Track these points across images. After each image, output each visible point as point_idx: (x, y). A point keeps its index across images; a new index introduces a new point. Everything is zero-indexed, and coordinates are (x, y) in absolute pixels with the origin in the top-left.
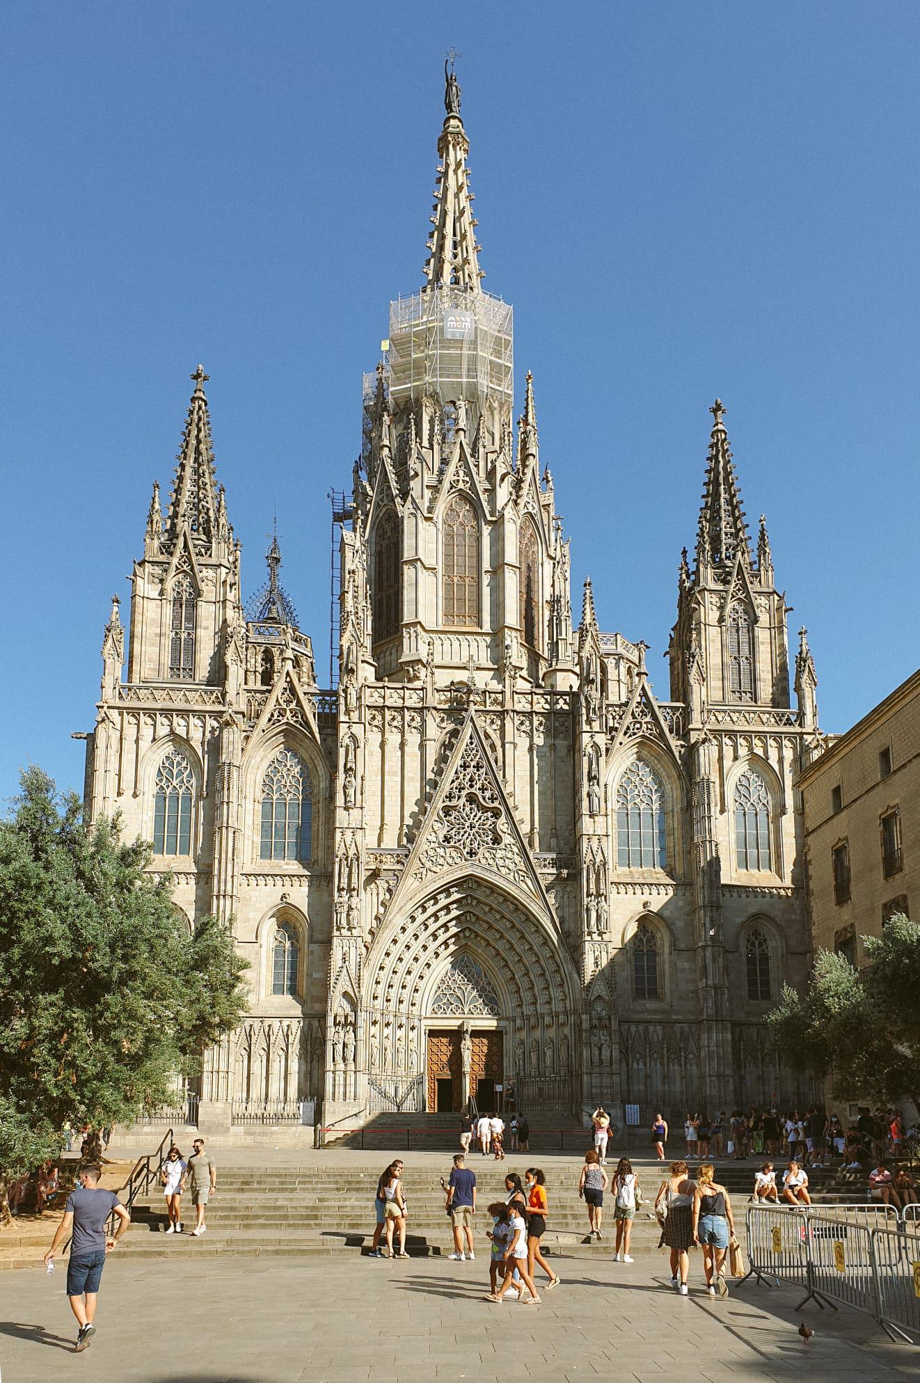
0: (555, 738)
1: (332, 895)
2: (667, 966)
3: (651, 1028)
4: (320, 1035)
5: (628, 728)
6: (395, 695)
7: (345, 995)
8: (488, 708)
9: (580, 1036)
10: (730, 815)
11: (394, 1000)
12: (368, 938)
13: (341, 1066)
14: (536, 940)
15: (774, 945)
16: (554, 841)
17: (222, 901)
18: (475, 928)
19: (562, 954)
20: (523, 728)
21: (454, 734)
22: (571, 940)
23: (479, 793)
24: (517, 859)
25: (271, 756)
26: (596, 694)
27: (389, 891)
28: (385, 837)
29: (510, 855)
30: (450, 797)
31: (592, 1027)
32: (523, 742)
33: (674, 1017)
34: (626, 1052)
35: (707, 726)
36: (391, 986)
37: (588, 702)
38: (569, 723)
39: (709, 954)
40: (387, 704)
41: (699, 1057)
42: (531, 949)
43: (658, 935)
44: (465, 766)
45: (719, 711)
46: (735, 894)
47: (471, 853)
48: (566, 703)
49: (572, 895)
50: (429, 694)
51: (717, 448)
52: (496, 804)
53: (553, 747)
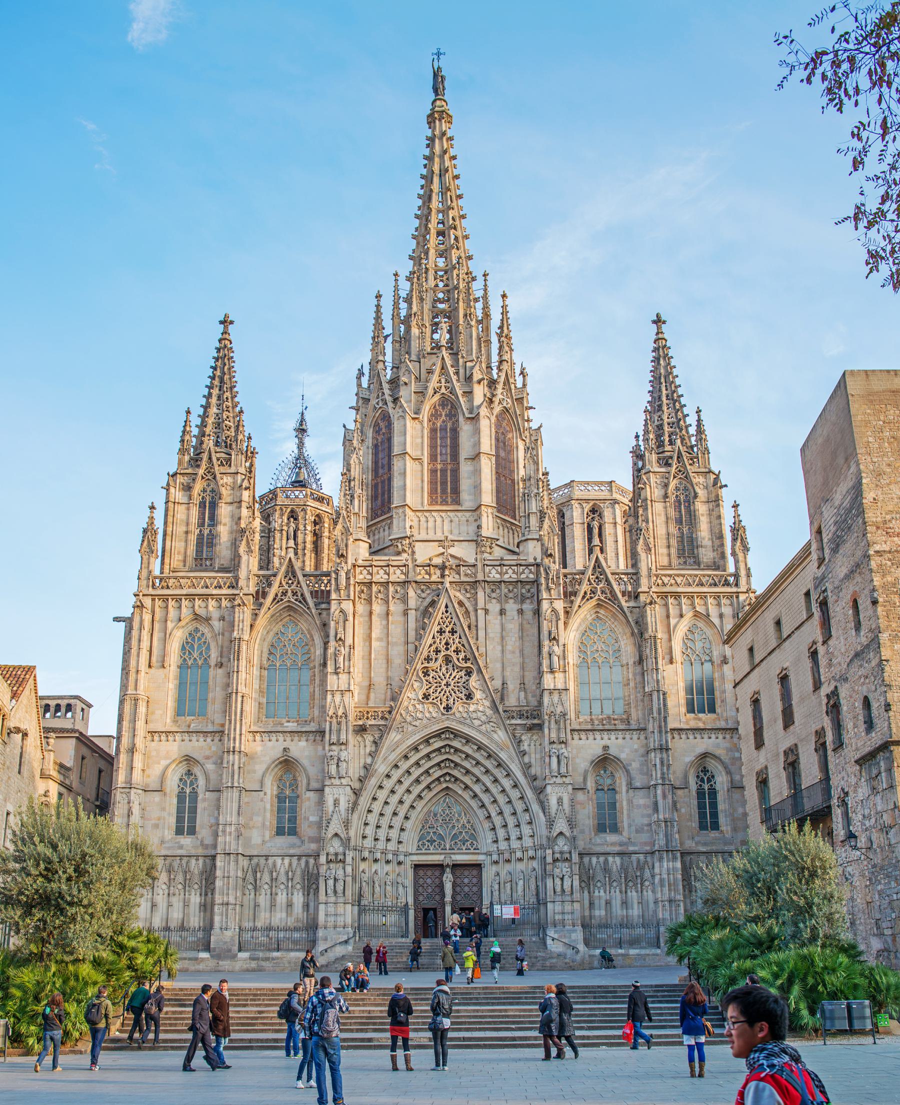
0: (522, 602)
1: (324, 749)
2: (625, 803)
3: (610, 859)
4: (315, 872)
5: (585, 593)
6: (381, 572)
7: (336, 835)
8: (464, 579)
9: (545, 869)
10: (678, 667)
11: (382, 838)
12: (357, 785)
13: (332, 899)
14: (507, 783)
15: (721, 781)
16: (522, 694)
17: (231, 756)
18: (455, 773)
19: (530, 794)
20: (494, 595)
21: (433, 603)
22: (538, 783)
23: (454, 655)
24: (489, 712)
25: (275, 630)
26: (555, 567)
27: (375, 742)
28: (372, 695)
29: (481, 709)
30: (428, 659)
31: (555, 860)
32: (494, 607)
33: (631, 848)
34: (587, 880)
35: (654, 589)
36: (378, 827)
37: (547, 574)
38: (534, 590)
39: (659, 792)
40: (374, 580)
41: (653, 884)
42: (503, 791)
43: (617, 775)
44: (441, 632)
45: (665, 575)
46: (684, 736)
47: (448, 708)
48: (531, 572)
49: (538, 744)
50: (411, 570)
53: (521, 612)
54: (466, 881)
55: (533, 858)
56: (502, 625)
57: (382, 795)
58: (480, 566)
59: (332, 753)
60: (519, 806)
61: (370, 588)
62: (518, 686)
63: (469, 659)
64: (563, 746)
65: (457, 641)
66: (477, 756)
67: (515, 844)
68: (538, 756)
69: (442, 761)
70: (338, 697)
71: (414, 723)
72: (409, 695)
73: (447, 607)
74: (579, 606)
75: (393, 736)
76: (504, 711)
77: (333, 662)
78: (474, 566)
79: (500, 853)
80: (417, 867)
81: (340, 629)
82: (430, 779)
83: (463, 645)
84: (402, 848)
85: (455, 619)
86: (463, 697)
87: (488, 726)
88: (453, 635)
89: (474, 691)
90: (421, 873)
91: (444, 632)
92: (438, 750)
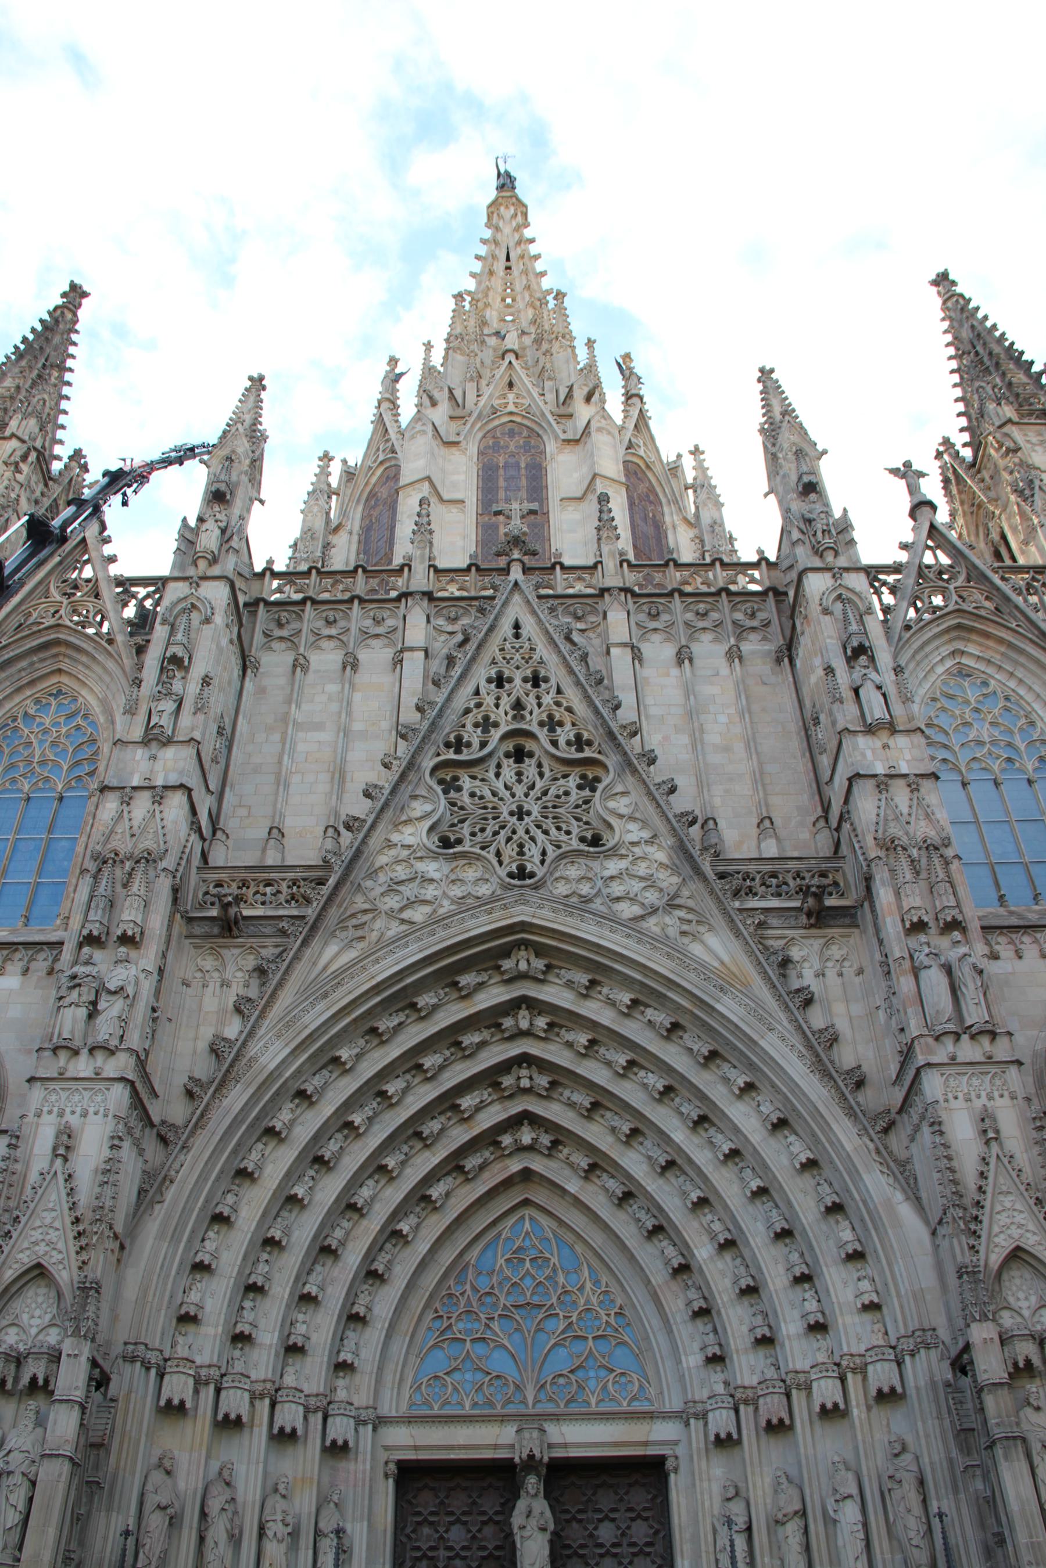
0: (739, 637)
7: (38, 1272)
11: (268, 1337)
14: (747, 1119)
18: (553, 1111)
23: (542, 734)
24: (668, 881)
27: (261, 971)
29: (642, 869)
32: (659, 651)
38: (769, 609)
44: (500, 681)
48: (753, 580)
49: (849, 971)
51: (959, 312)
52: (588, 753)
54: (606, 1533)
55: (887, 1397)
56: (688, 691)
57: (275, 1164)
58: (610, 564)
59: (80, 969)
60: (804, 1200)
61: (300, 617)
62: (755, 832)
63: (589, 743)
64: (956, 935)
65: (547, 700)
66: (633, 1029)
67: (799, 1352)
68: (857, 1009)
69: (506, 1067)
70: (142, 804)
71: (405, 915)
72: (395, 837)
73: (517, 626)
74: (908, 627)
75: (331, 954)
76: (722, 876)
77: (141, 718)
78: (594, 567)
79: (740, 1401)
80: (412, 1476)
81: (179, 637)
82: (460, 1135)
83: (569, 710)
84: (356, 1392)
85: (543, 650)
86: (575, 844)
87: (668, 920)
88: (536, 684)
89: (614, 821)
90: (426, 1502)
91: (510, 680)
92: (490, 1019)
